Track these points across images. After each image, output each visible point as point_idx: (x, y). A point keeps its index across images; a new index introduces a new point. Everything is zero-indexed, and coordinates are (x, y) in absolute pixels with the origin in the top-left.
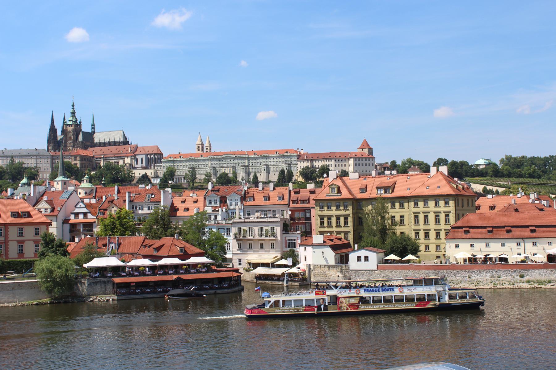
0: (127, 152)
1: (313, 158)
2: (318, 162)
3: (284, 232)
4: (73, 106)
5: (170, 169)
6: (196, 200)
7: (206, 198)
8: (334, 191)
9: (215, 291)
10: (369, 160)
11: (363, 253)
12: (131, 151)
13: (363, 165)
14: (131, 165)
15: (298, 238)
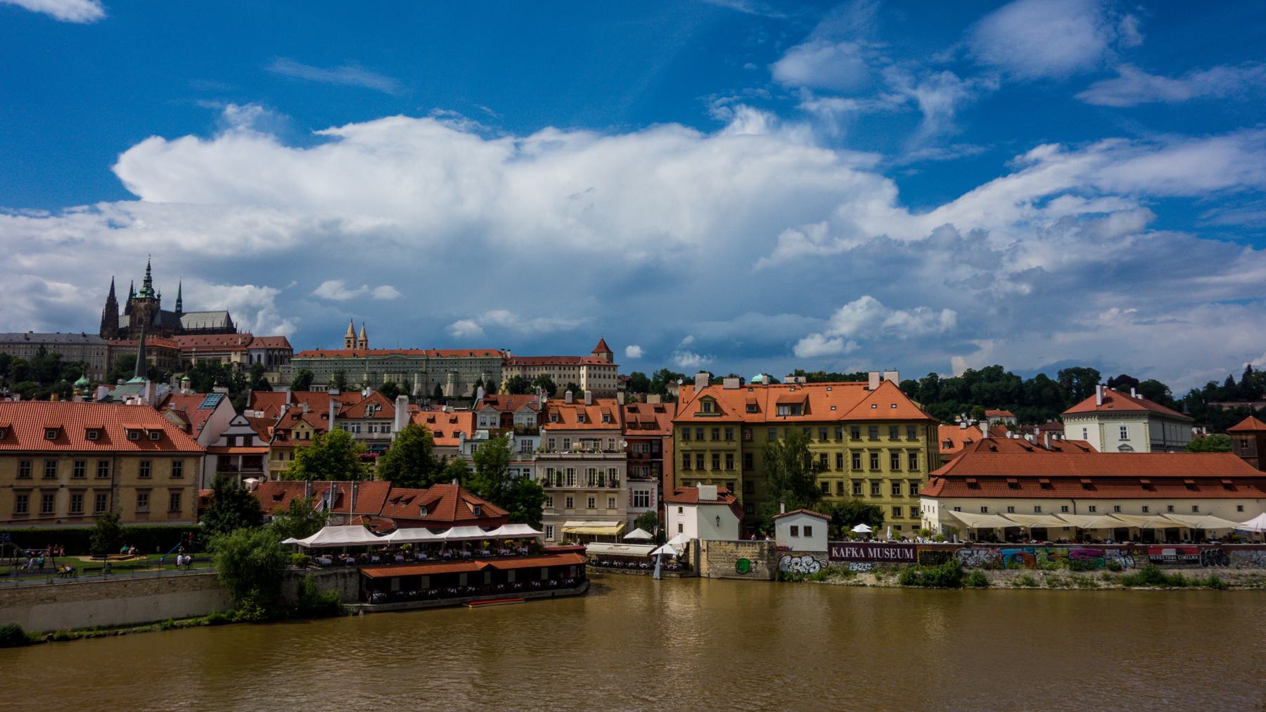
0: (236, 344)
1: (526, 363)
2: (534, 370)
3: (629, 478)
4: (149, 269)
5: (305, 373)
6: (454, 418)
7: (476, 415)
8: (709, 409)
9: (552, 591)
10: (609, 370)
11: (802, 521)
12: (242, 343)
13: (595, 377)
14: (239, 364)
15: (653, 489)
